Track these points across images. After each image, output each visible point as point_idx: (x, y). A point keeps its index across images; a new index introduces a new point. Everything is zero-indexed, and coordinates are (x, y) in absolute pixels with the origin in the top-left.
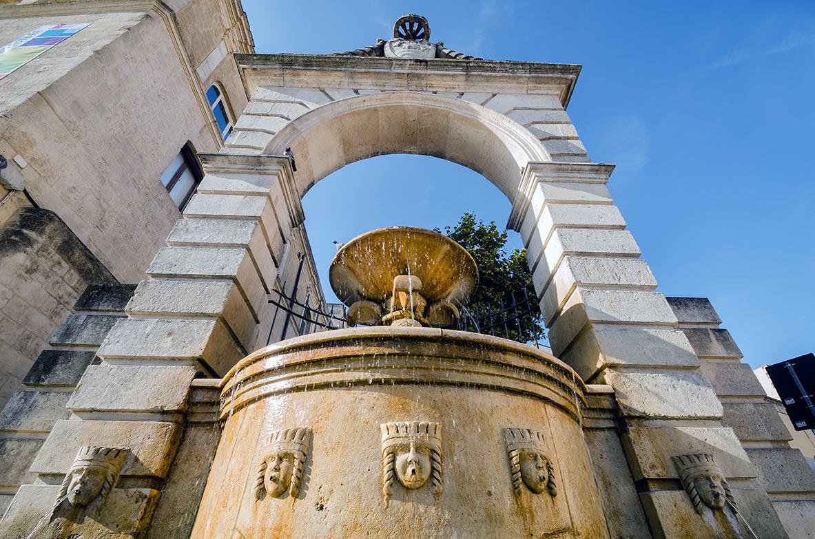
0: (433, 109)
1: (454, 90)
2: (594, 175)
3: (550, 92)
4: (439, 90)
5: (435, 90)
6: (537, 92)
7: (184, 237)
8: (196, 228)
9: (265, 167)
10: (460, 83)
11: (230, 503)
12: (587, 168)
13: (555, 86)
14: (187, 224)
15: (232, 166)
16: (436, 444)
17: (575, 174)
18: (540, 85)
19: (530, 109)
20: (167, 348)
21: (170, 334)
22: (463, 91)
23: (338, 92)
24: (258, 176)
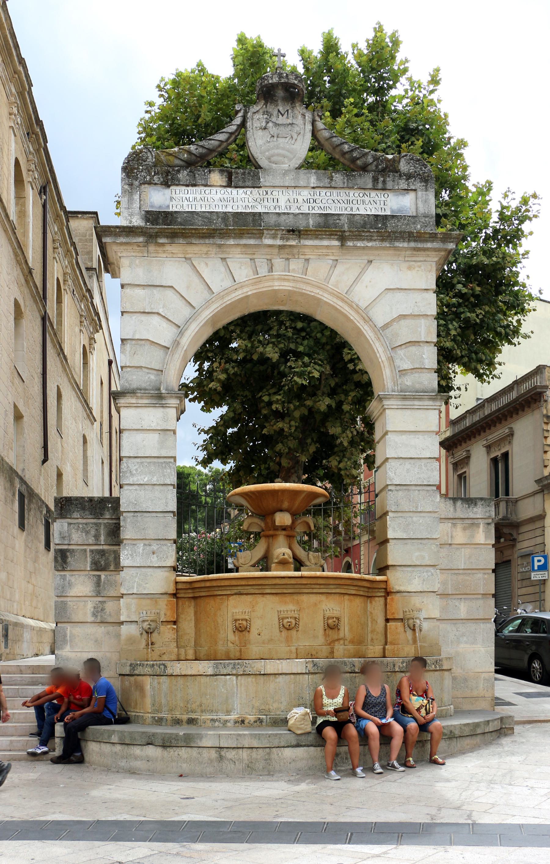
0: (304, 293)
1: (328, 257)
2: (431, 403)
3: (429, 259)
4: (311, 257)
5: (307, 257)
6: (414, 259)
7: (131, 480)
8: (136, 470)
9: (167, 402)
10: (333, 251)
11: (222, 632)
12: (426, 397)
13: (434, 253)
14: (128, 467)
15: (140, 401)
16: (297, 616)
17: (416, 403)
18: (419, 253)
19: (402, 289)
20: (155, 561)
21: (153, 553)
22: (337, 258)
23: (207, 264)
24: (161, 410)
